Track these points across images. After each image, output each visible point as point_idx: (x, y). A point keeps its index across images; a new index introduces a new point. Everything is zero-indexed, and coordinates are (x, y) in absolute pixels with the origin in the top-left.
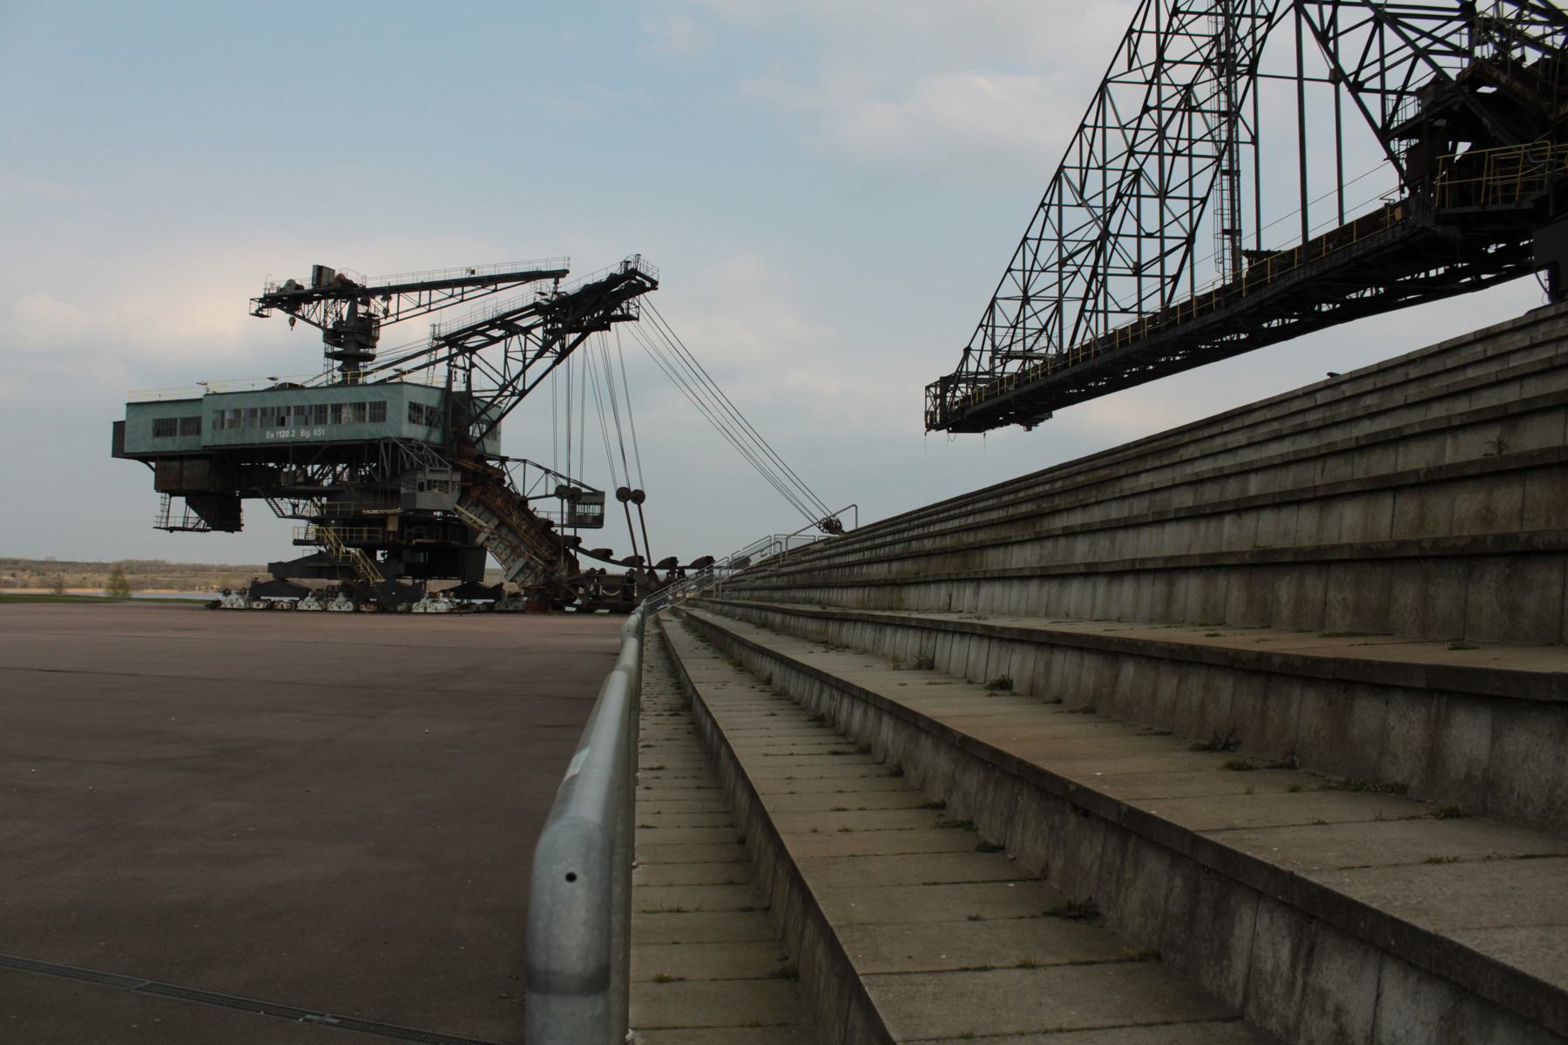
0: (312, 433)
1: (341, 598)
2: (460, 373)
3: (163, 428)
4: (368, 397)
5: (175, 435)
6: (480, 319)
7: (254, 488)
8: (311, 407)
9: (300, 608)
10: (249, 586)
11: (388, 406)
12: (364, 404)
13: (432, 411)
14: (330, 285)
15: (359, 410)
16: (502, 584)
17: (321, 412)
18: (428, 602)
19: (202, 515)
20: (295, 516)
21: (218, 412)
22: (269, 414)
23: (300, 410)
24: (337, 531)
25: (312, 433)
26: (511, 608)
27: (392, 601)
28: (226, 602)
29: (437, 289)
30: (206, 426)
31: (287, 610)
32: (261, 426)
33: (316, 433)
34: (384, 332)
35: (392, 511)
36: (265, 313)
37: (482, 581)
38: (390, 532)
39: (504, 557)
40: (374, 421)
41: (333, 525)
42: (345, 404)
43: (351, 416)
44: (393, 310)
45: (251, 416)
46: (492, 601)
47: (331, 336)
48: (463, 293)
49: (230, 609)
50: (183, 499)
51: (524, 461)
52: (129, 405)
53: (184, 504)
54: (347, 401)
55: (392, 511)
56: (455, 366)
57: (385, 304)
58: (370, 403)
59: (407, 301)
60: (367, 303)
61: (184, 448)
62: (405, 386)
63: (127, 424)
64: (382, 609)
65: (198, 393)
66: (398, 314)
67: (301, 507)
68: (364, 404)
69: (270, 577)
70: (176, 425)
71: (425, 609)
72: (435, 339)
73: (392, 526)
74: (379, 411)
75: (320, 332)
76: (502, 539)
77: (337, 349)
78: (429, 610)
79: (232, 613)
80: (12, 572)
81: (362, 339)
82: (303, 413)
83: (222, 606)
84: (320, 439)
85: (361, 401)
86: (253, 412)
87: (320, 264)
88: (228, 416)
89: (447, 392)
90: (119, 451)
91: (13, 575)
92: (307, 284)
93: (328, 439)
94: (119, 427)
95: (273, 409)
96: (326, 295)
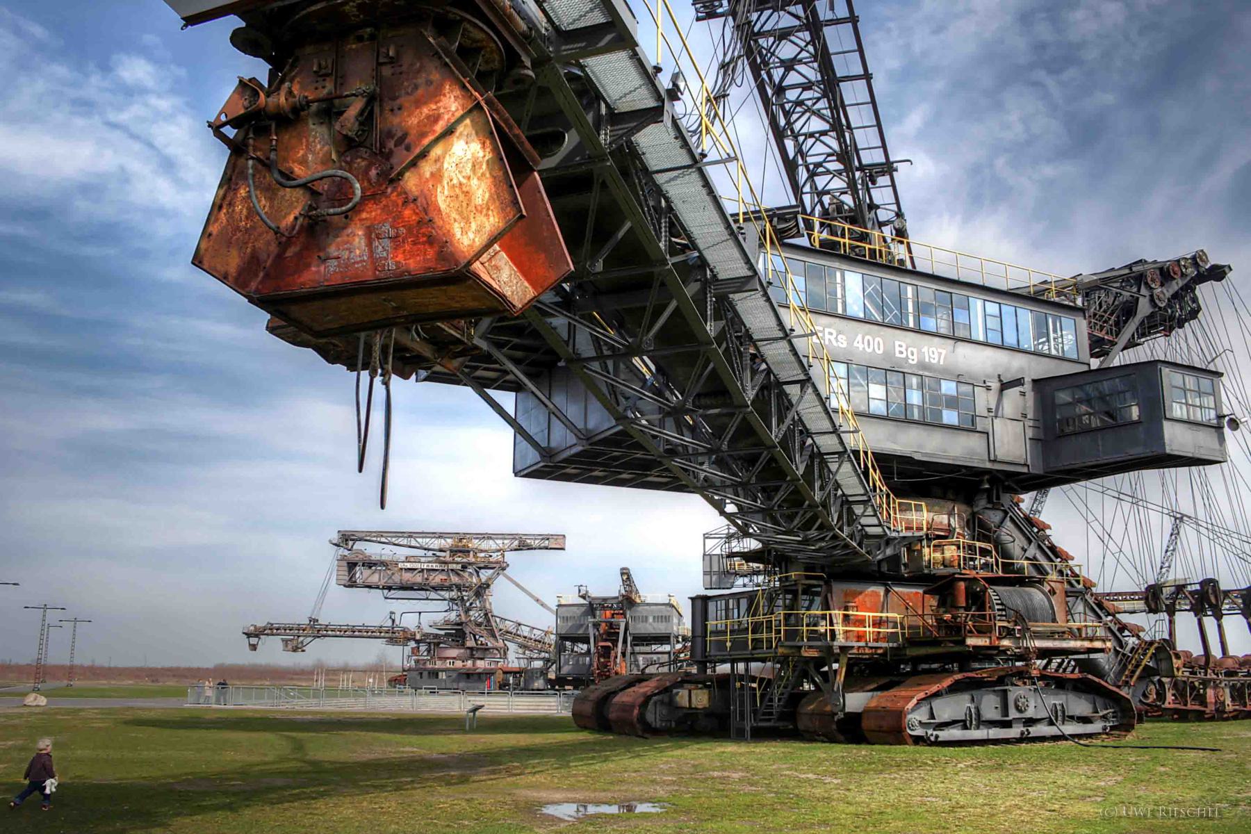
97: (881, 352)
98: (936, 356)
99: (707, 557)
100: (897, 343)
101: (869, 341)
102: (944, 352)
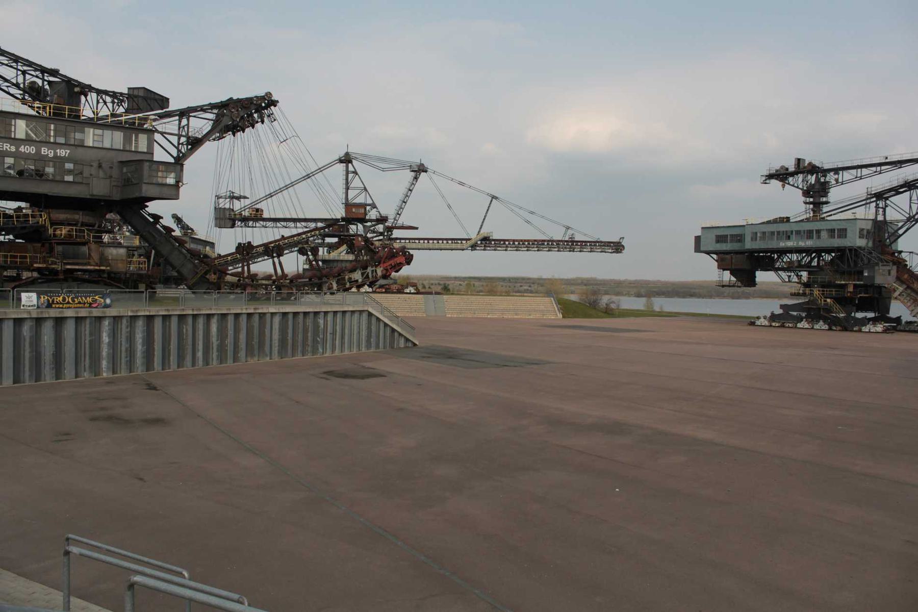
0: (805, 243)
1: (821, 323)
2: (881, 210)
3: (720, 239)
4: (836, 226)
5: (727, 242)
6: (895, 184)
7: (769, 268)
8: (804, 231)
9: (798, 327)
10: (770, 315)
11: (848, 231)
12: (834, 230)
13: (868, 232)
14: (803, 168)
15: (831, 232)
16: (901, 316)
17: (810, 233)
18: (871, 326)
19: (738, 280)
20: (789, 281)
21: (754, 233)
22: (781, 234)
23: (798, 232)
24: (819, 291)
25: (805, 243)
26: (907, 329)
27: (847, 326)
28: (758, 323)
29: (866, 168)
30: (748, 238)
31: (791, 327)
32: (777, 240)
33: (809, 243)
34: (832, 190)
35: (850, 282)
36: (767, 182)
37: (888, 314)
38: (848, 292)
39: (909, 304)
40: (840, 238)
41: (816, 287)
42: (824, 230)
43: (826, 236)
44: (840, 180)
45: (772, 235)
46: (895, 325)
47: (806, 193)
48: (881, 171)
49: (760, 326)
50: (729, 272)
51: (912, 252)
52: (702, 228)
53: (730, 275)
54: (825, 228)
55: (850, 282)
56: (879, 207)
57: (836, 176)
58: (838, 229)
59: (847, 175)
60: (825, 176)
61: (731, 249)
62: (858, 220)
63: (702, 237)
64: (845, 329)
65: (745, 224)
66: (842, 182)
67: (792, 277)
68: (834, 230)
69: (781, 311)
70: (727, 238)
71: (869, 330)
72: (868, 195)
73: (851, 289)
74: (843, 233)
75: (800, 192)
76: (909, 295)
77: (808, 200)
78: (872, 331)
79: (764, 327)
80: (528, 284)
81: (822, 194)
82: (800, 234)
83: (756, 324)
84: (810, 246)
85: (833, 228)
86: (773, 233)
87: (799, 158)
88: (759, 235)
89: (875, 221)
90: (698, 249)
91: (530, 286)
92: (792, 169)
93: (814, 247)
94: (698, 239)
95: (783, 232)
96: (801, 173)
97: (33, 152)
98: (64, 153)
99: (217, 210)
100: (43, 149)
101: (27, 148)
102: (68, 151)
